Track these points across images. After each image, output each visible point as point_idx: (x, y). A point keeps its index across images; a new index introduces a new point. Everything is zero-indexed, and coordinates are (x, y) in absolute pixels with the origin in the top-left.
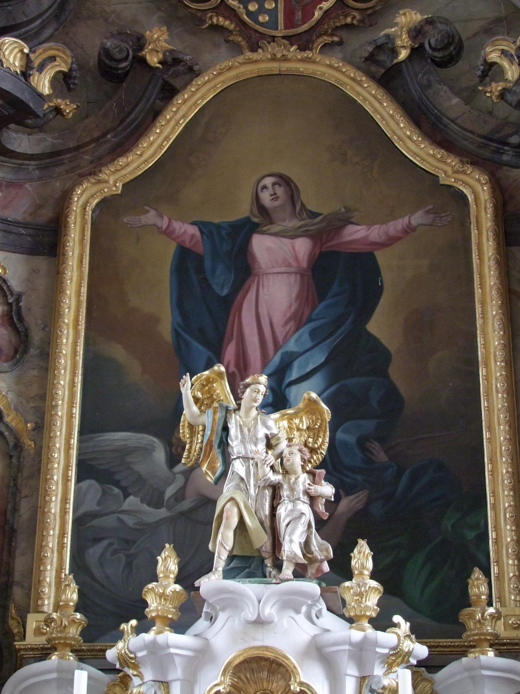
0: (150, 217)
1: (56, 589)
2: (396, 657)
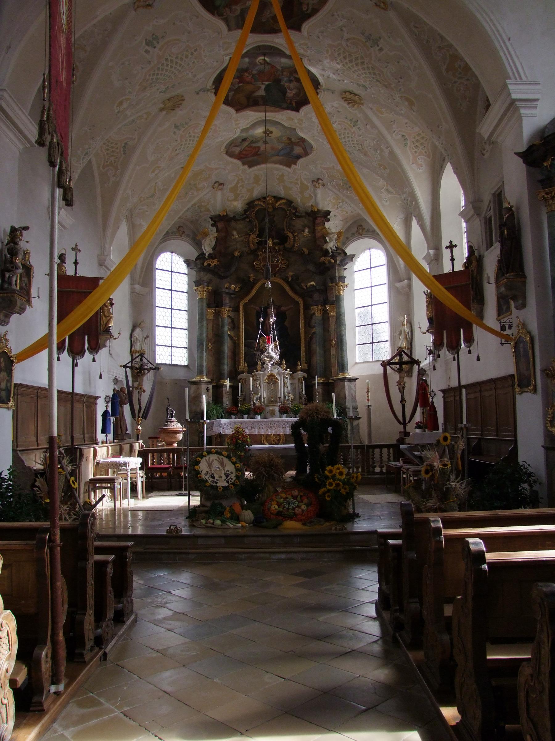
0: (252, 306)
1: (243, 365)
2: (288, 374)
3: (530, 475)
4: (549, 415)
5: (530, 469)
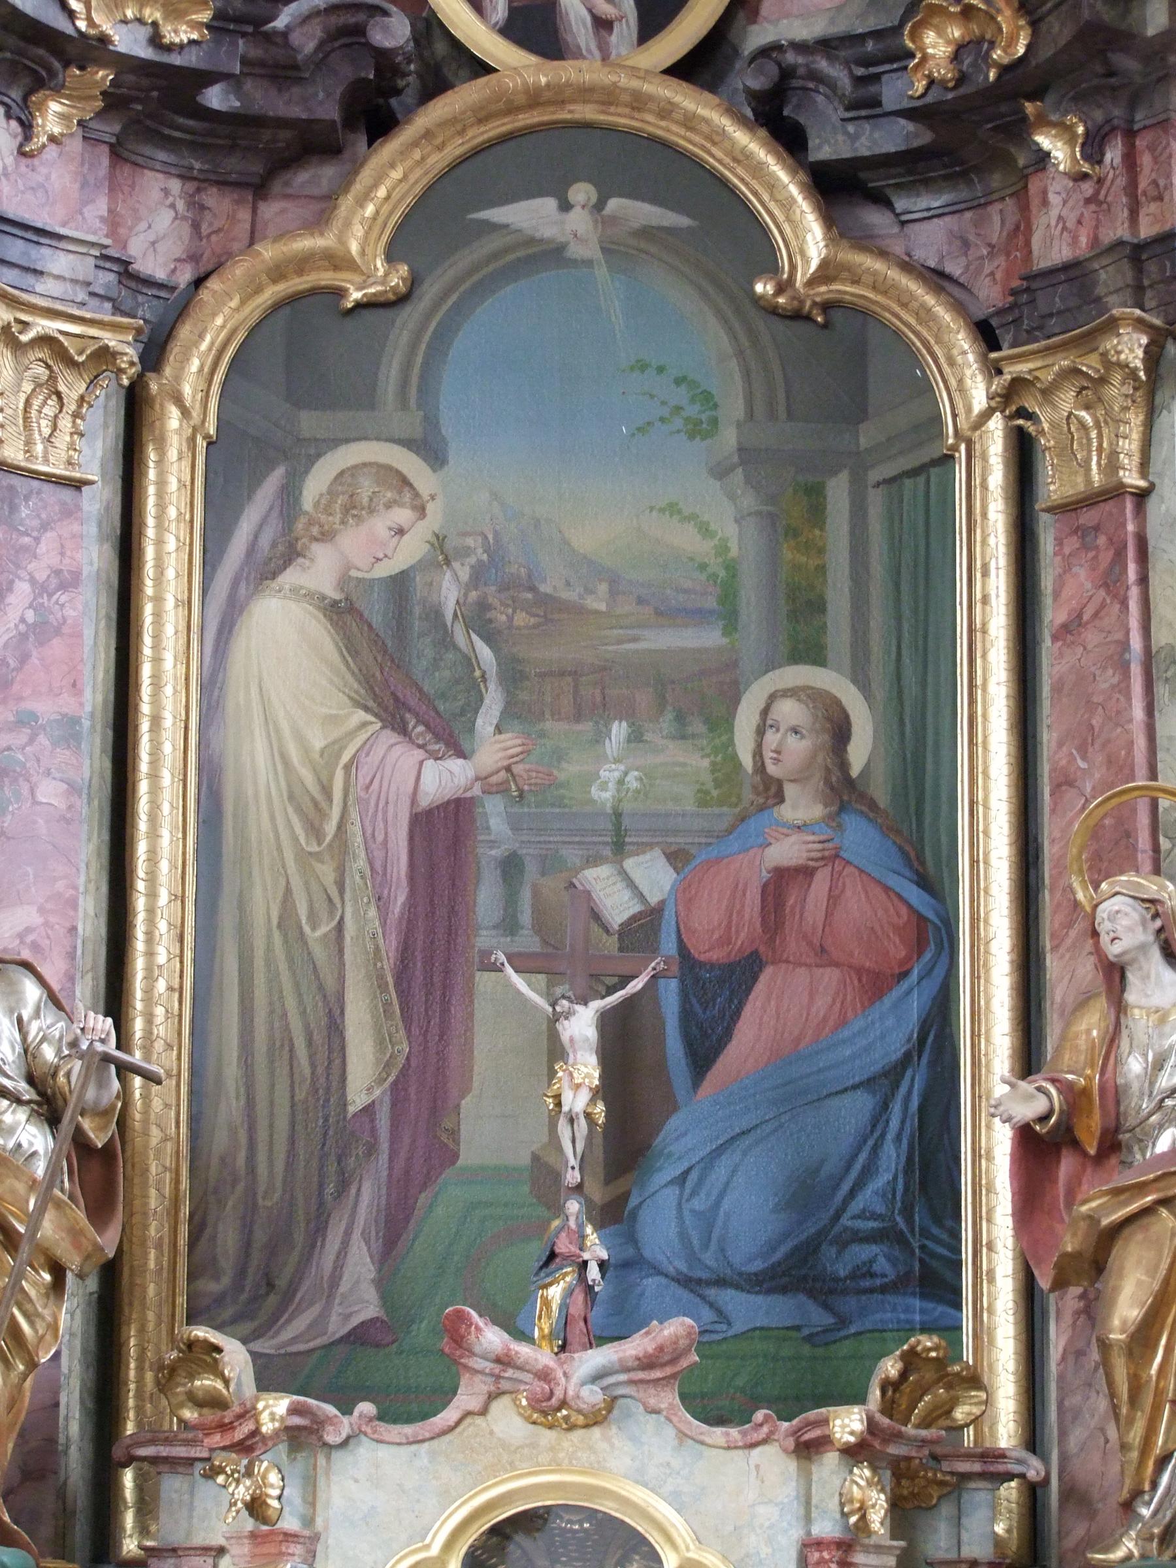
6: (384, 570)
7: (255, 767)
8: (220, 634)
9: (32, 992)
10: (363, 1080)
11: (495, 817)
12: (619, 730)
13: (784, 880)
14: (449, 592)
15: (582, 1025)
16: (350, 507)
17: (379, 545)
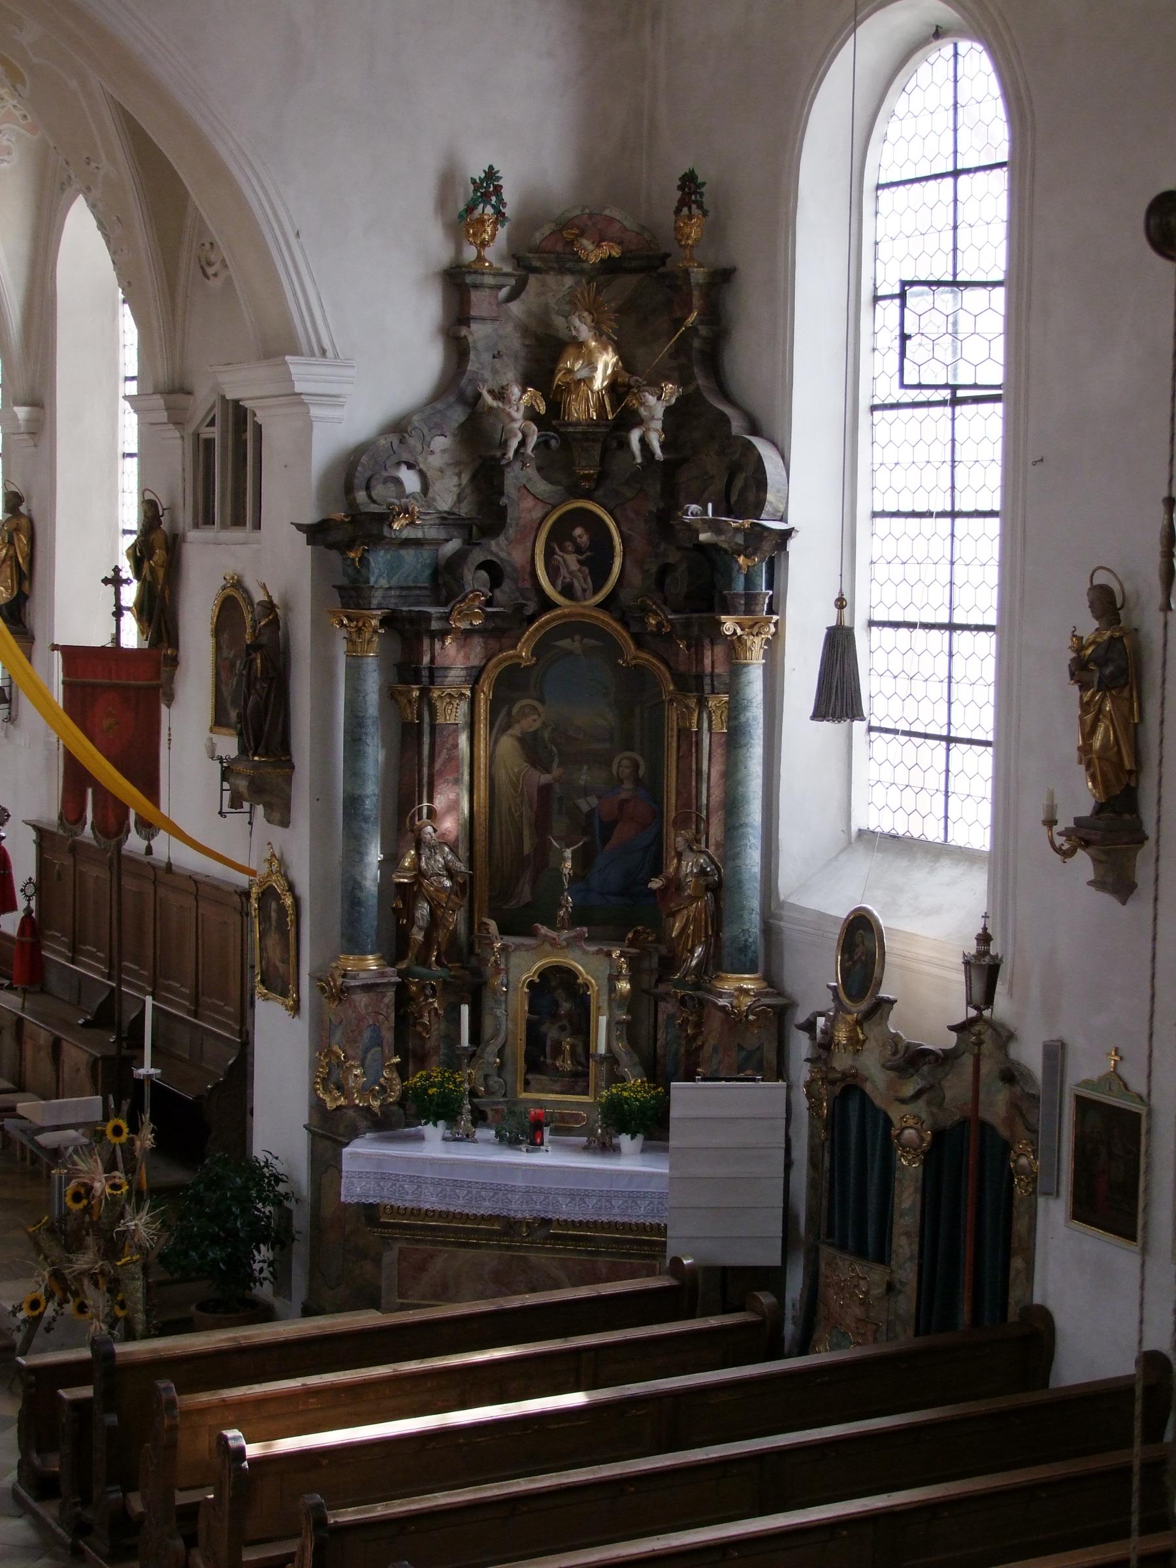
3: (277, 1179)
4: (322, 1067)
5: (280, 1168)
6: (531, 730)
7: (502, 776)
8: (494, 743)
9: (447, 849)
10: (527, 848)
11: (557, 786)
12: (585, 767)
13: (622, 804)
14: (546, 736)
15: (568, 853)
16: (523, 714)
17: (530, 723)
